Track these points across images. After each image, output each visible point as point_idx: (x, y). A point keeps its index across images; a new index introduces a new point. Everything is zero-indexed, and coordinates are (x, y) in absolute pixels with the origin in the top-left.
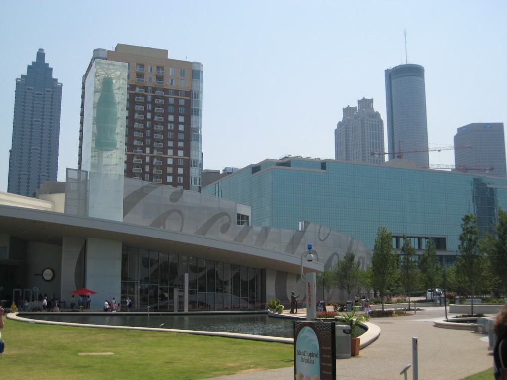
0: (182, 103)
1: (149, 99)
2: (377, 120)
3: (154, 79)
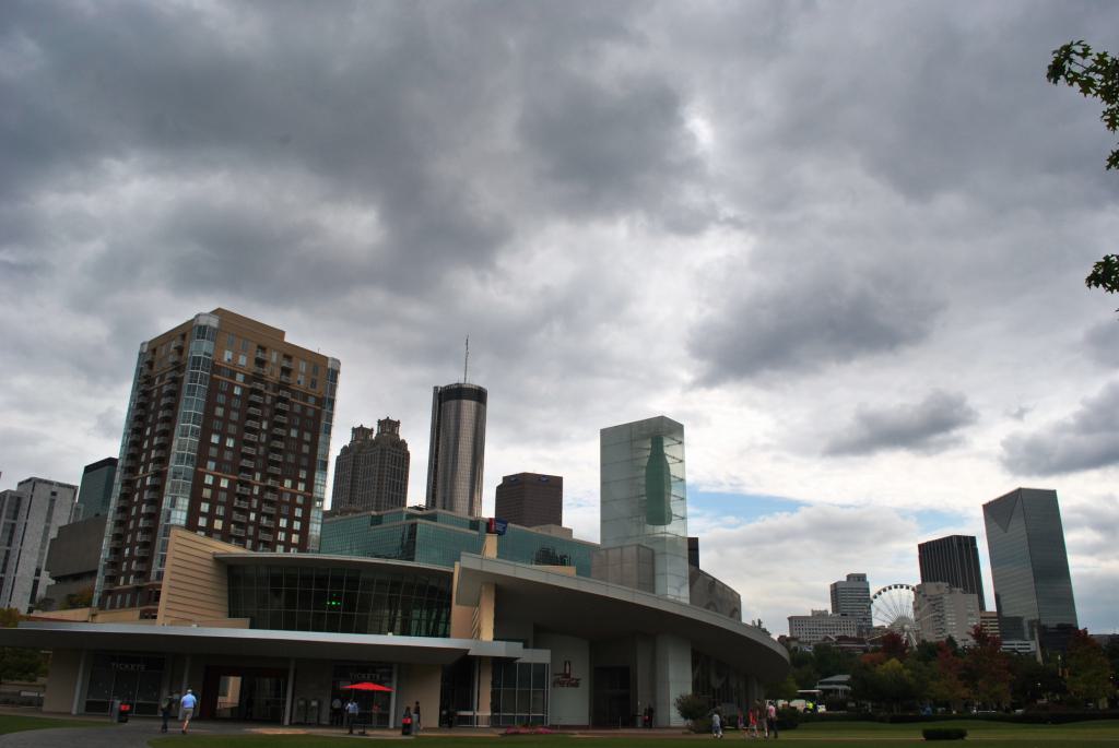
0: (310, 413)
1: (269, 400)
3: (277, 372)
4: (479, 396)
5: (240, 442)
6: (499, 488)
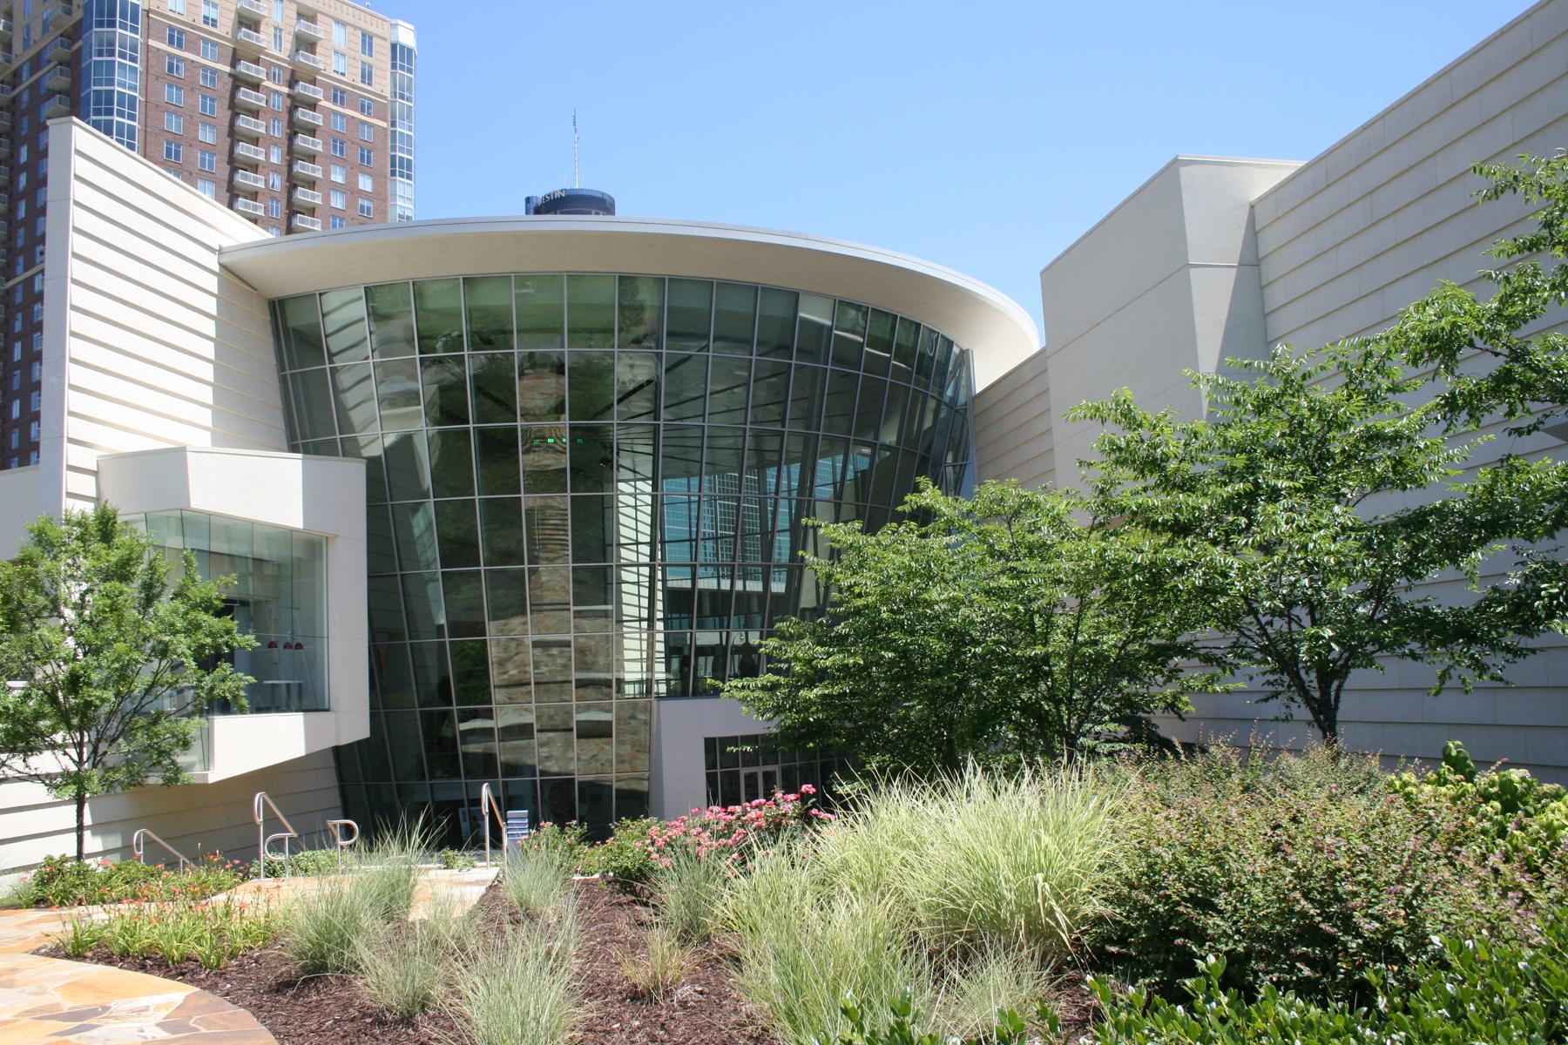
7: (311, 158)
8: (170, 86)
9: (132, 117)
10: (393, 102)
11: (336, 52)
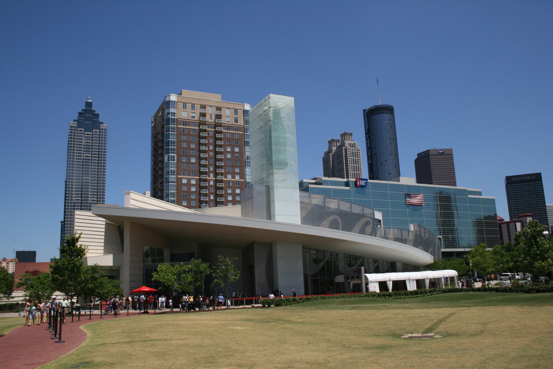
1: (211, 134)
2: (356, 149)
4: (389, 110)
5: (200, 159)
6: (416, 160)
7: (221, 146)
8: (184, 136)
9: (174, 146)
10: (244, 126)
11: (227, 117)
